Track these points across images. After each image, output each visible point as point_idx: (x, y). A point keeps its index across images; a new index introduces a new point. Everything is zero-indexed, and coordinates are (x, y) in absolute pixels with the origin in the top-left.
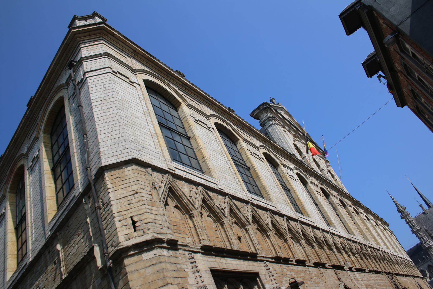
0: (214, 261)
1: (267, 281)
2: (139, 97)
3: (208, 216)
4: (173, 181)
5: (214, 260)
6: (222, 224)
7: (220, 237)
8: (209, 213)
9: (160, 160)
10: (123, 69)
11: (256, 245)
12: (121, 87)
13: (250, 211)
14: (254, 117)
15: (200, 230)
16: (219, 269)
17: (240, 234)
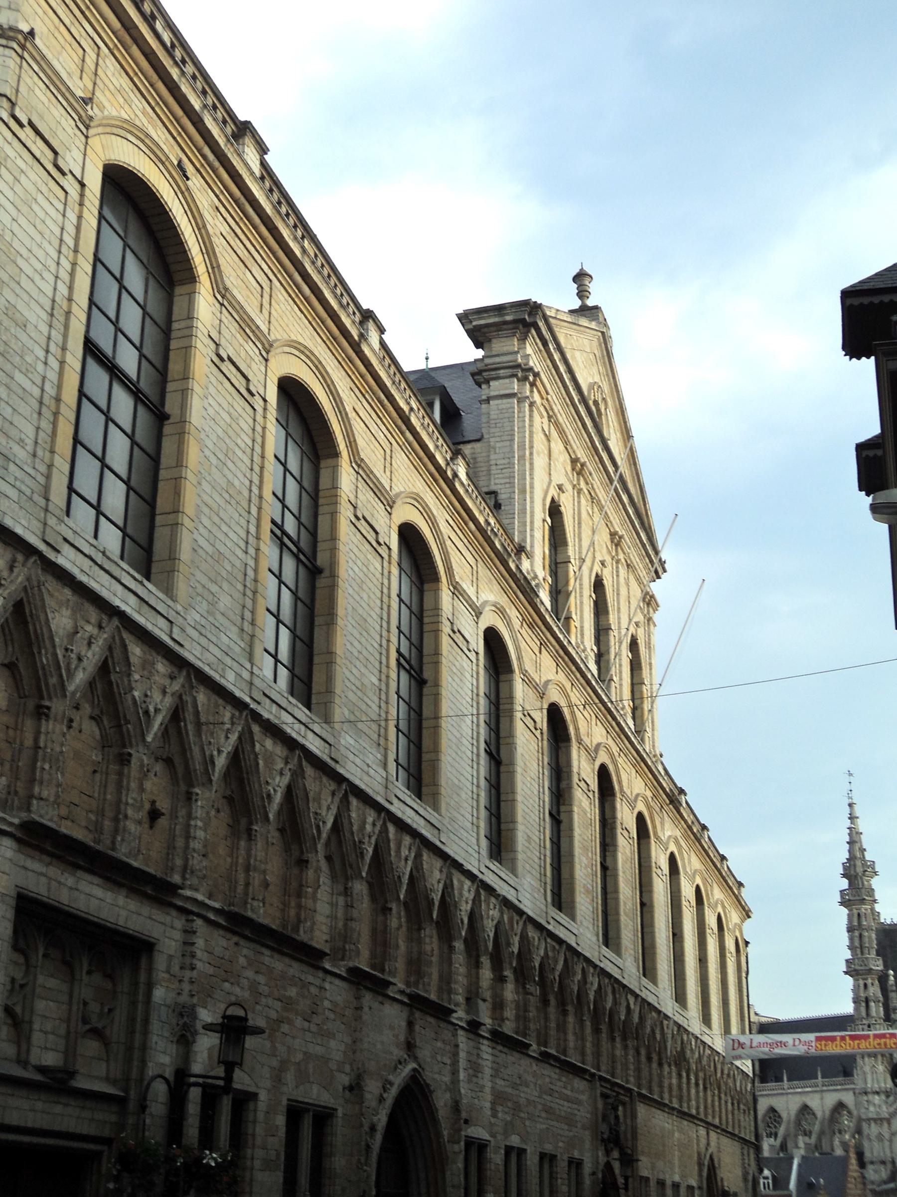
0: (42, 874)
1: (166, 976)
2: (61, 240)
3: (92, 718)
4: (39, 587)
5: (44, 870)
6: (124, 760)
7: (96, 795)
8: (102, 712)
9: (27, 505)
10: (53, 110)
11: (195, 855)
12: (18, 188)
13: (234, 737)
14: (467, 331)
15: (47, 766)
16: (45, 899)
17: (164, 805)
